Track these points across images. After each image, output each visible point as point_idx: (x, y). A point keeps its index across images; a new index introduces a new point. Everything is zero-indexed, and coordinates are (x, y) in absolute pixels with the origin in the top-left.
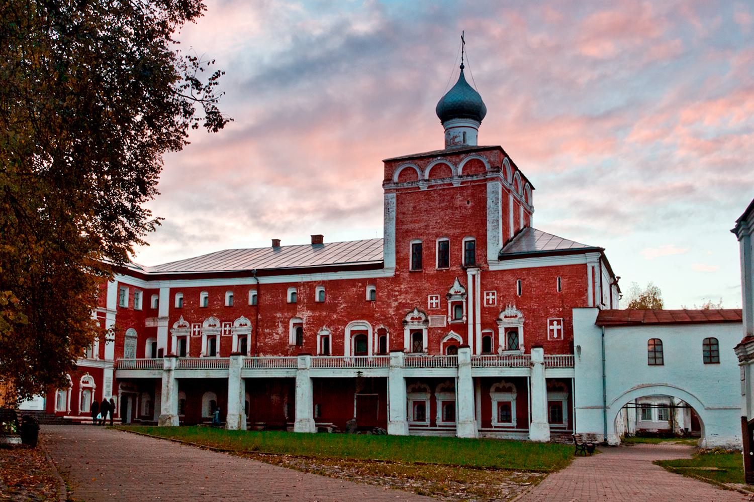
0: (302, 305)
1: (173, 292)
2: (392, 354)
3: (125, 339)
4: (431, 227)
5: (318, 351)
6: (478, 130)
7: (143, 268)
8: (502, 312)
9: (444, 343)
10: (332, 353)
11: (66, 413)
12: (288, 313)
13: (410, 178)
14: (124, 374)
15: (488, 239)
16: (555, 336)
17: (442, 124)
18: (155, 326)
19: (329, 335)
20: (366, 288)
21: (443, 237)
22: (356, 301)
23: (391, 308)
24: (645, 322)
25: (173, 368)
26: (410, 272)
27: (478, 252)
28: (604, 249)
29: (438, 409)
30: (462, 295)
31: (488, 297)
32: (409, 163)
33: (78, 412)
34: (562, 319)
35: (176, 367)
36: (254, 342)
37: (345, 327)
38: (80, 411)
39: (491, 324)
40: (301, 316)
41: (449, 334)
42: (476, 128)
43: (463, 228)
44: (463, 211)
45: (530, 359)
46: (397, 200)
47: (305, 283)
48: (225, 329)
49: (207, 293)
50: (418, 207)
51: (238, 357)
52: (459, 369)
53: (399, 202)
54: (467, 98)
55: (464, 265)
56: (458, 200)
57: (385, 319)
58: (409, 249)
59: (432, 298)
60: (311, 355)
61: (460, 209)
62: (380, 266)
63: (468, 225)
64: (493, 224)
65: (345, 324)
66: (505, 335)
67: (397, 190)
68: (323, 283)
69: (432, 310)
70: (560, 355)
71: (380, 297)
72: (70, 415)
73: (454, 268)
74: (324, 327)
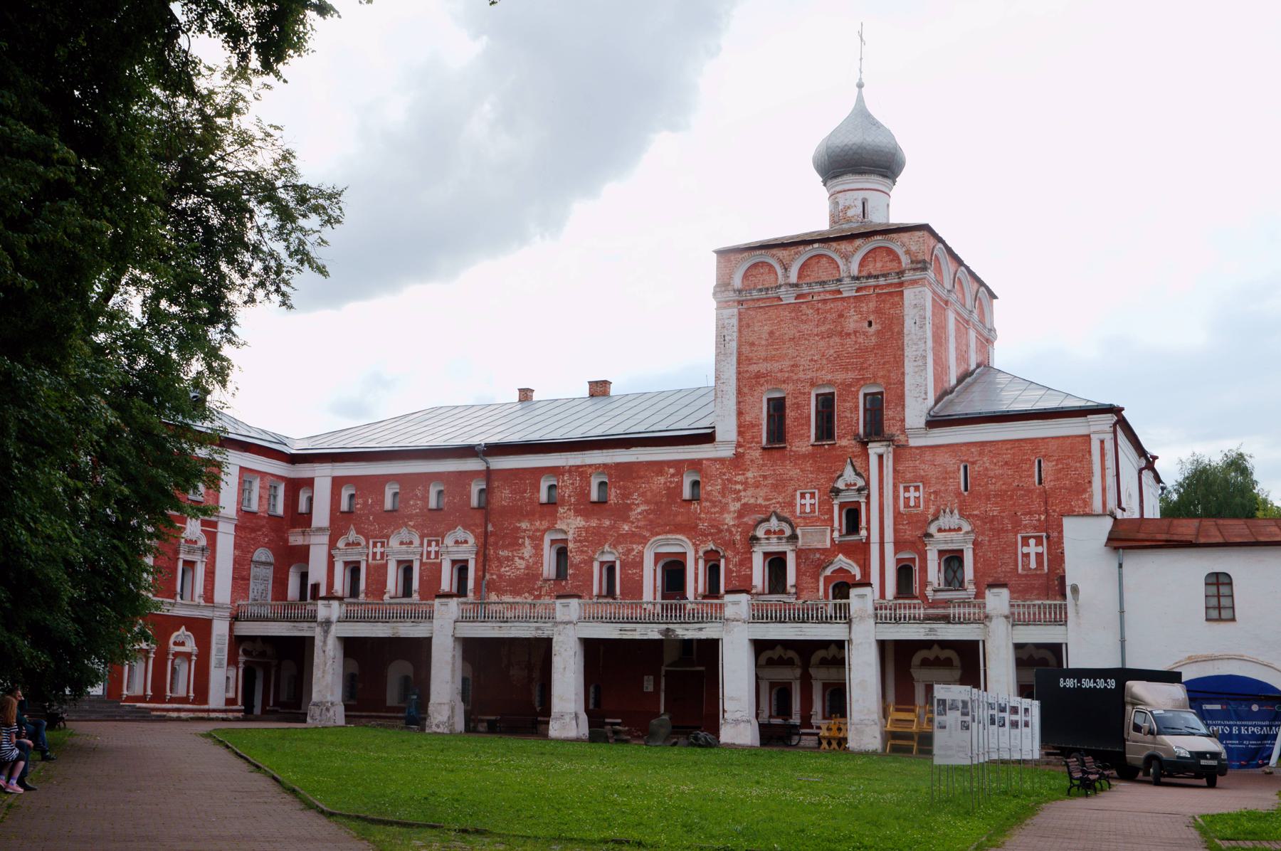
0: (566, 508)
1: (337, 483)
2: (729, 598)
3: (252, 566)
4: (801, 368)
5: (595, 591)
6: (891, 194)
7: (286, 441)
8: (932, 521)
9: (826, 578)
10: (621, 594)
11: (142, 699)
12: (541, 521)
13: (764, 280)
14: (246, 629)
15: (906, 389)
16: (1033, 565)
17: (825, 185)
18: (305, 543)
19: (615, 562)
20: (682, 476)
21: (823, 385)
22: (664, 500)
24: (1202, 540)
25: (334, 618)
26: (764, 449)
27: (888, 413)
28: (1122, 409)
29: (814, 697)
30: (859, 490)
31: (907, 495)
32: (762, 254)
33: (165, 696)
34: (1045, 534)
35: (339, 617)
36: (480, 573)
37: (644, 548)
38: (168, 693)
39: (913, 543)
40: (564, 527)
41: (836, 560)
42: (887, 190)
43: (860, 370)
44: (860, 340)
45: (985, 607)
46: (740, 320)
47: (573, 469)
48: (429, 549)
49: (397, 486)
51: (449, 600)
52: (854, 627)
53: (743, 325)
54: (871, 139)
55: (862, 437)
56: (851, 320)
57: (717, 530)
58: (761, 408)
59: (803, 496)
60: (579, 597)
61: (856, 336)
62: (707, 438)
63: (870, 365)
64: (916, 364)
65: (644, 541)
66: (939, 564)
67: (740, 303)
68: (605, 467)
69: (805, 518)
70: (1040, 602)
71: (709, 493)
72: (151, 701)
73: (844, 442)
74: (607, 548)
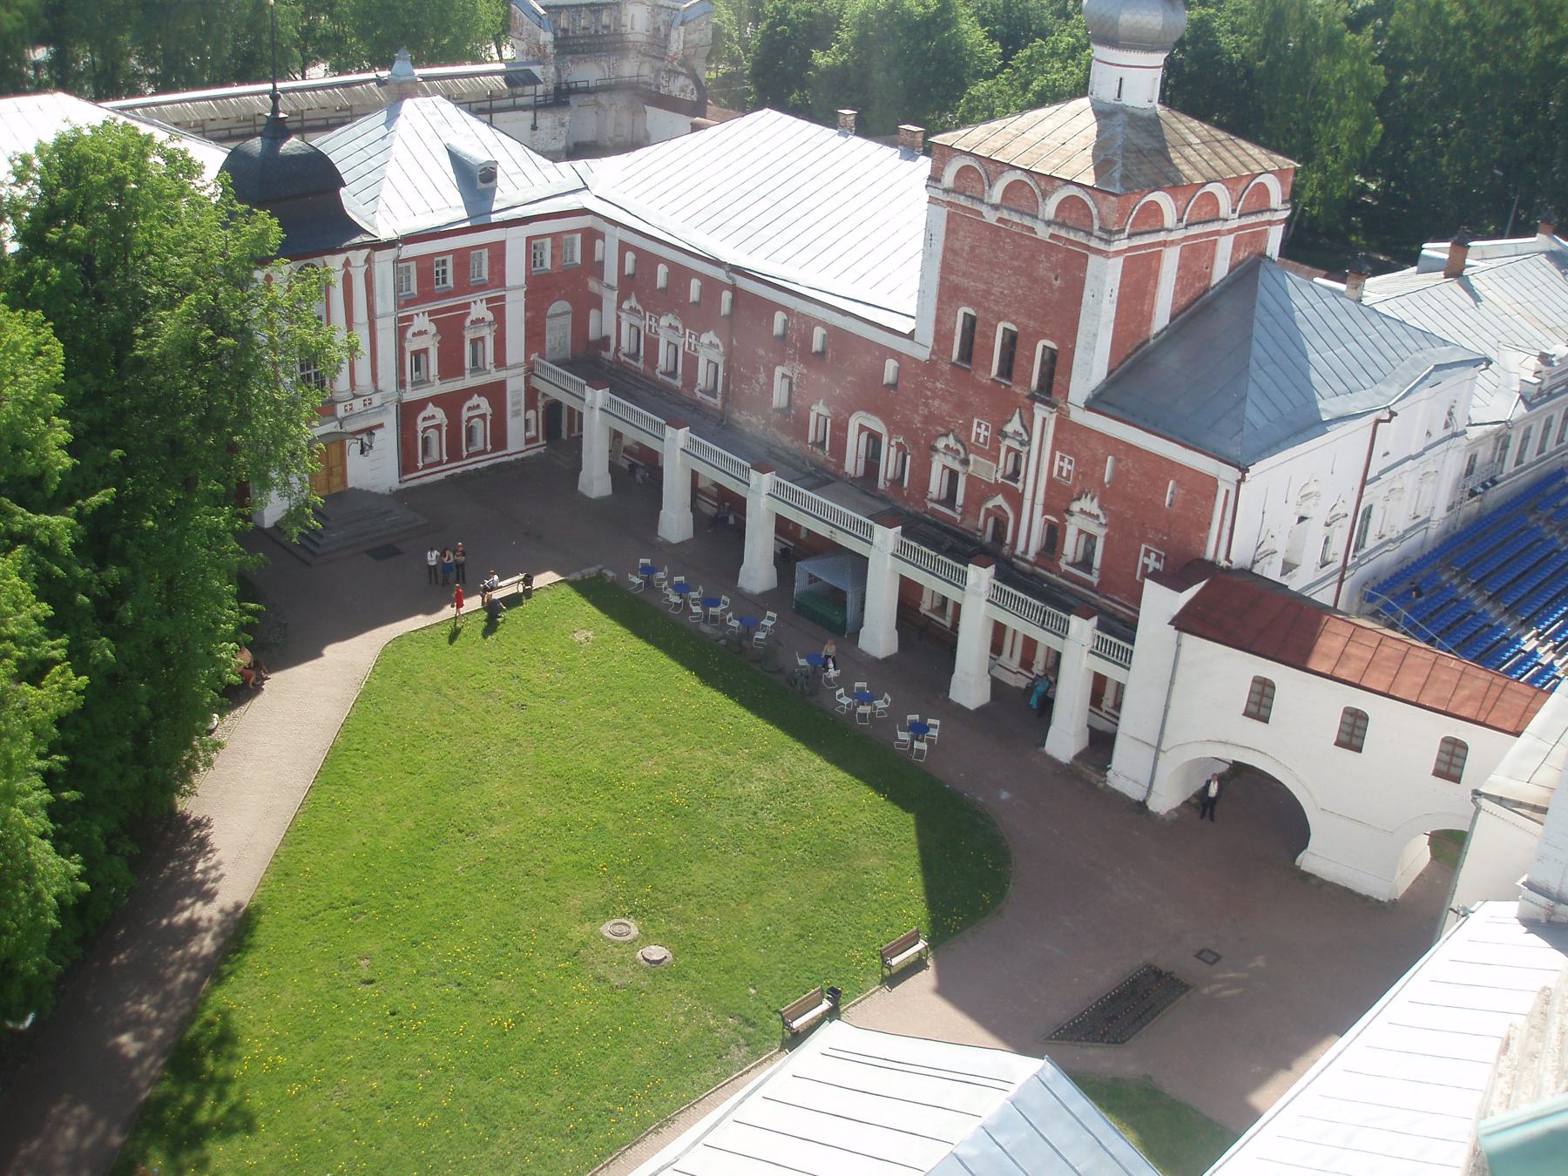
23: (918, 414)
50: (977, 251)
53: (950, 231)
63: (1050, 321)
